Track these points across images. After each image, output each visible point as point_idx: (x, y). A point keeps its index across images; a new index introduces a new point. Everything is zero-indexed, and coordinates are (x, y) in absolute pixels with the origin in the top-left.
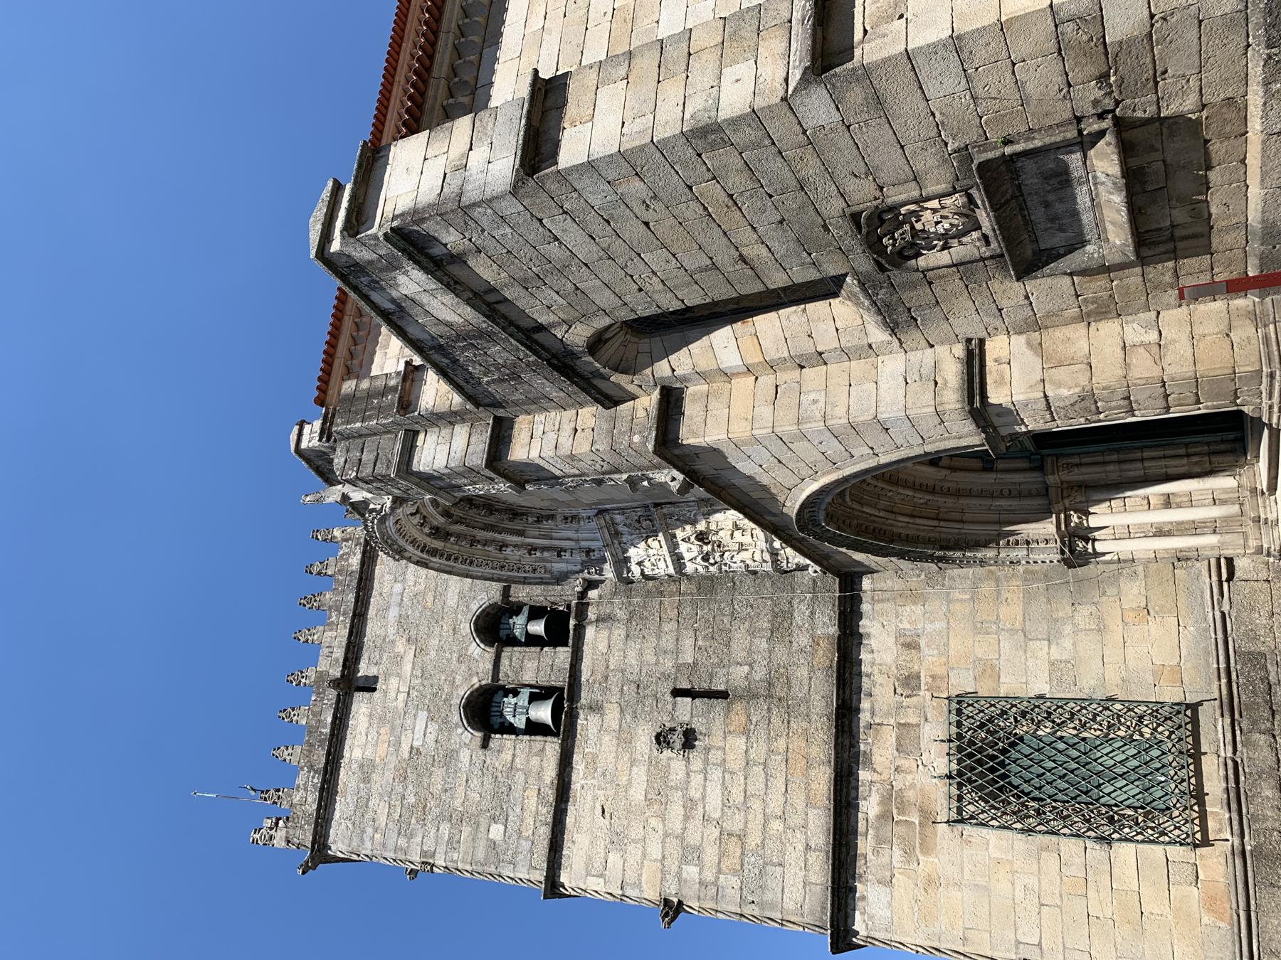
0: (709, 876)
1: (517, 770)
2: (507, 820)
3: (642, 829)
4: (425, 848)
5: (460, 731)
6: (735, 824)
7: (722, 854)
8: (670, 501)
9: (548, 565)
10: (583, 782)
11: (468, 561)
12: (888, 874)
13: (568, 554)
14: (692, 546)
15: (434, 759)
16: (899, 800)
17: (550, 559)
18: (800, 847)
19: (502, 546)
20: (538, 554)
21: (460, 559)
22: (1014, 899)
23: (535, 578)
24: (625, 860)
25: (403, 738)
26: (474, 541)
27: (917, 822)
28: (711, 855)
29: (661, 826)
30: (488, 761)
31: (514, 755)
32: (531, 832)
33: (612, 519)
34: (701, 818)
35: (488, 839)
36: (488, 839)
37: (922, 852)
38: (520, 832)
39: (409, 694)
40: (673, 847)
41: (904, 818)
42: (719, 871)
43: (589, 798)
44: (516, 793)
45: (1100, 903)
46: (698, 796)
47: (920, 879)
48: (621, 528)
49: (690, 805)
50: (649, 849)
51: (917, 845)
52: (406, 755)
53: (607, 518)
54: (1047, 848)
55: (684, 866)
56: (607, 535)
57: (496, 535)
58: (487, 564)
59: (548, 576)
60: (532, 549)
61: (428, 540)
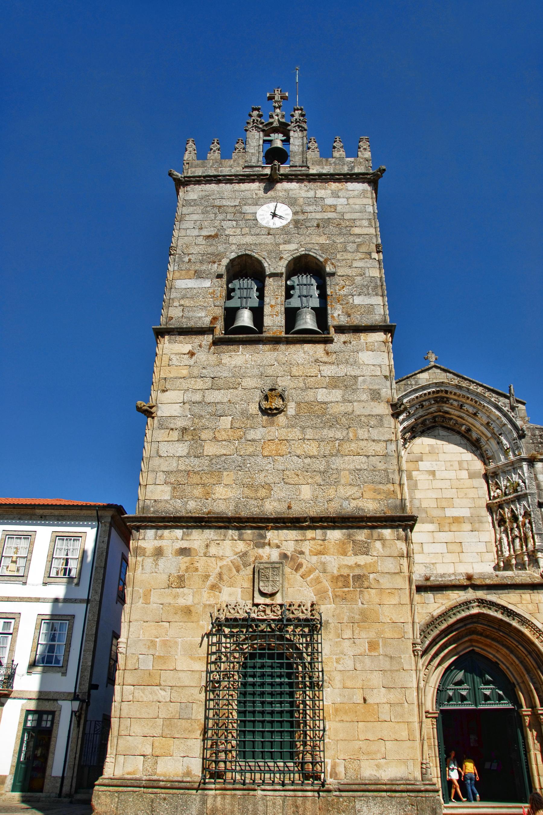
57: (415, 417)
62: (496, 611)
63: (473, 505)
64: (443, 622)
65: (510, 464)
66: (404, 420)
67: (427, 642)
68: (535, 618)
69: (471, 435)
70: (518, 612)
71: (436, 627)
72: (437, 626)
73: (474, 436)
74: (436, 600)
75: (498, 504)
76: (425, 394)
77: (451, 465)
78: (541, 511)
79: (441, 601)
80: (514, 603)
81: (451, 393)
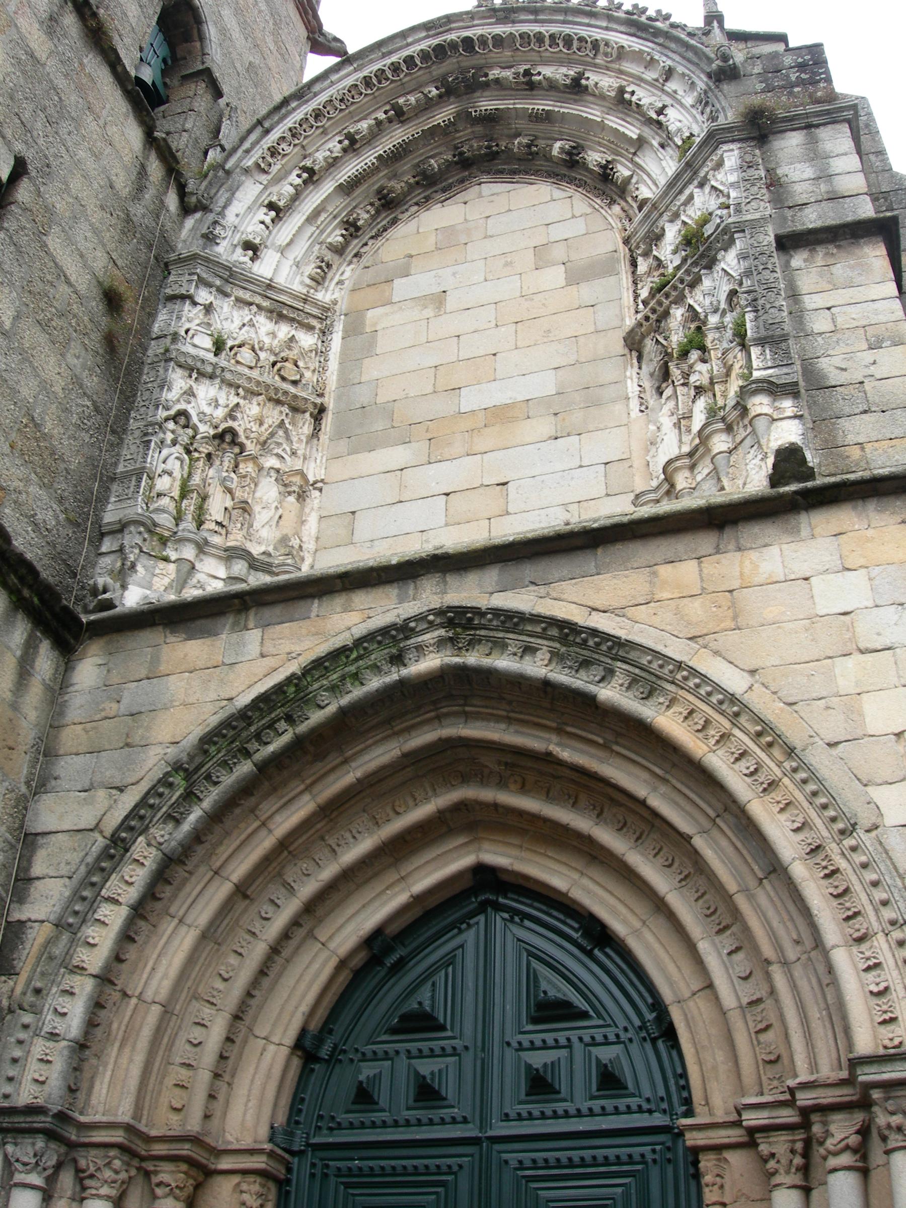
8: (324, 437)
9: (264, 178)
11: (374, 80)
13: (268, 220)
14: (220, 413)
17: (275, 189)
19: (353, 144)
20: (298, 181)
21: (389, 74)
23: (257, 142)
26: (400, 115)
33: (310, 328)
48: (284, 331)
53: (314, 322)
56: (283, 298)
58: (342, 100)
59: (249, 162)
60: (312, 177)
61: (467, 61)
62: (529, 650)
63: (572, 359)
64: (282, 725)
65: (687, 176)
66: (333, 163)
67: (195, 815)
68: (716, 653)
69: (584, 166)
70: (622, 634)
71: (248, 754)
72: (253, 746)
73: (594, 157)
74: (269, 648)
75: (654, 317)
76: (395, 68)
77: (507, 264)
78: (787, 266)
79: (287, 646)
80: (616, 604)
81: (483, 40)
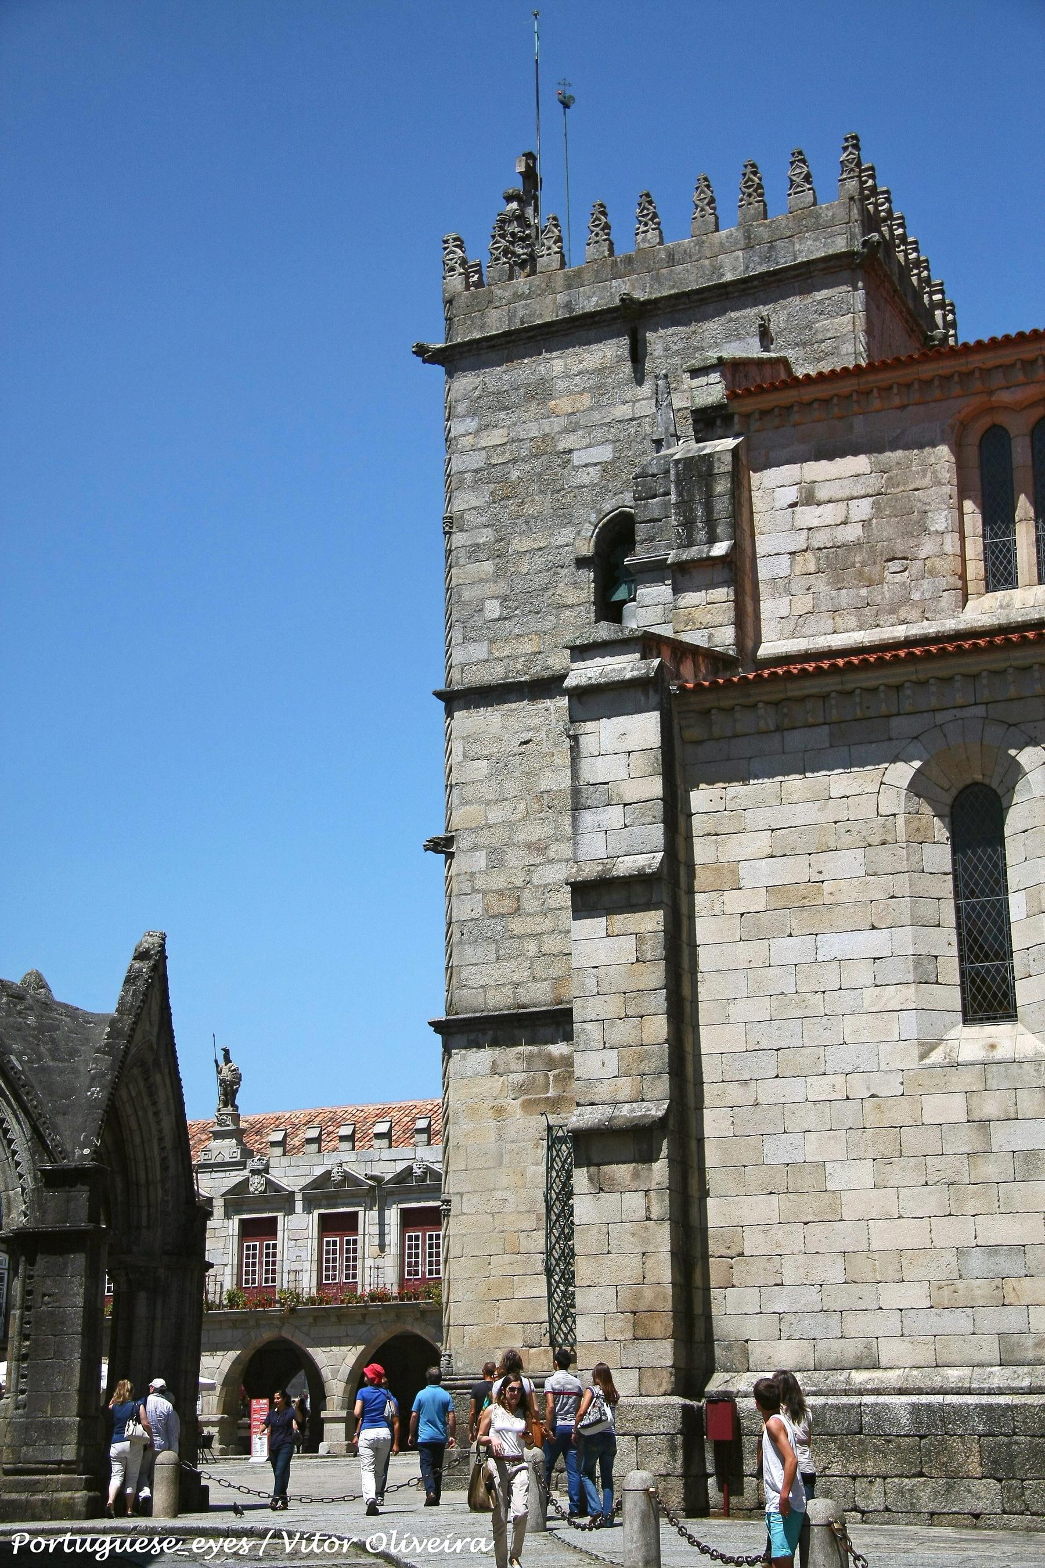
0: (479, 883)
1: (557, 617)
2: (505, 619)
3: (513, 795)
4: (466, 516)
5: (593, 518)
6: (530, 904)
7: (500, 893)
10: (552, 708)
12: (501, 1070)
15: (560, 491)
16: (567, 1075)
18: (516, 977)
22: (494, 1189)
24: (482, 781)
25: (580, 433)
27: (549, 1095)
28: (498, 881)
29: (519, 816)
30: (563, 572)
31: (573, 606)
32: (497, 654)
34: (532, 863)
35: (483, 600)
36: (483, 600)
37: (524, 1102)
38: (492, 641)
39: (632, 420)
40: (499, 836)
41: (551, 1082)
42: (485, 893)
43: (537, 721)
44: (534, 623)
45: (501, 1265)
46: (551, 854)
47: (500, 1101)
49: (538, 847)
50: (495, 808)
51: (530, 1097)
52: (561, 446)
54: (539, 1219)
55: (484, 853)
